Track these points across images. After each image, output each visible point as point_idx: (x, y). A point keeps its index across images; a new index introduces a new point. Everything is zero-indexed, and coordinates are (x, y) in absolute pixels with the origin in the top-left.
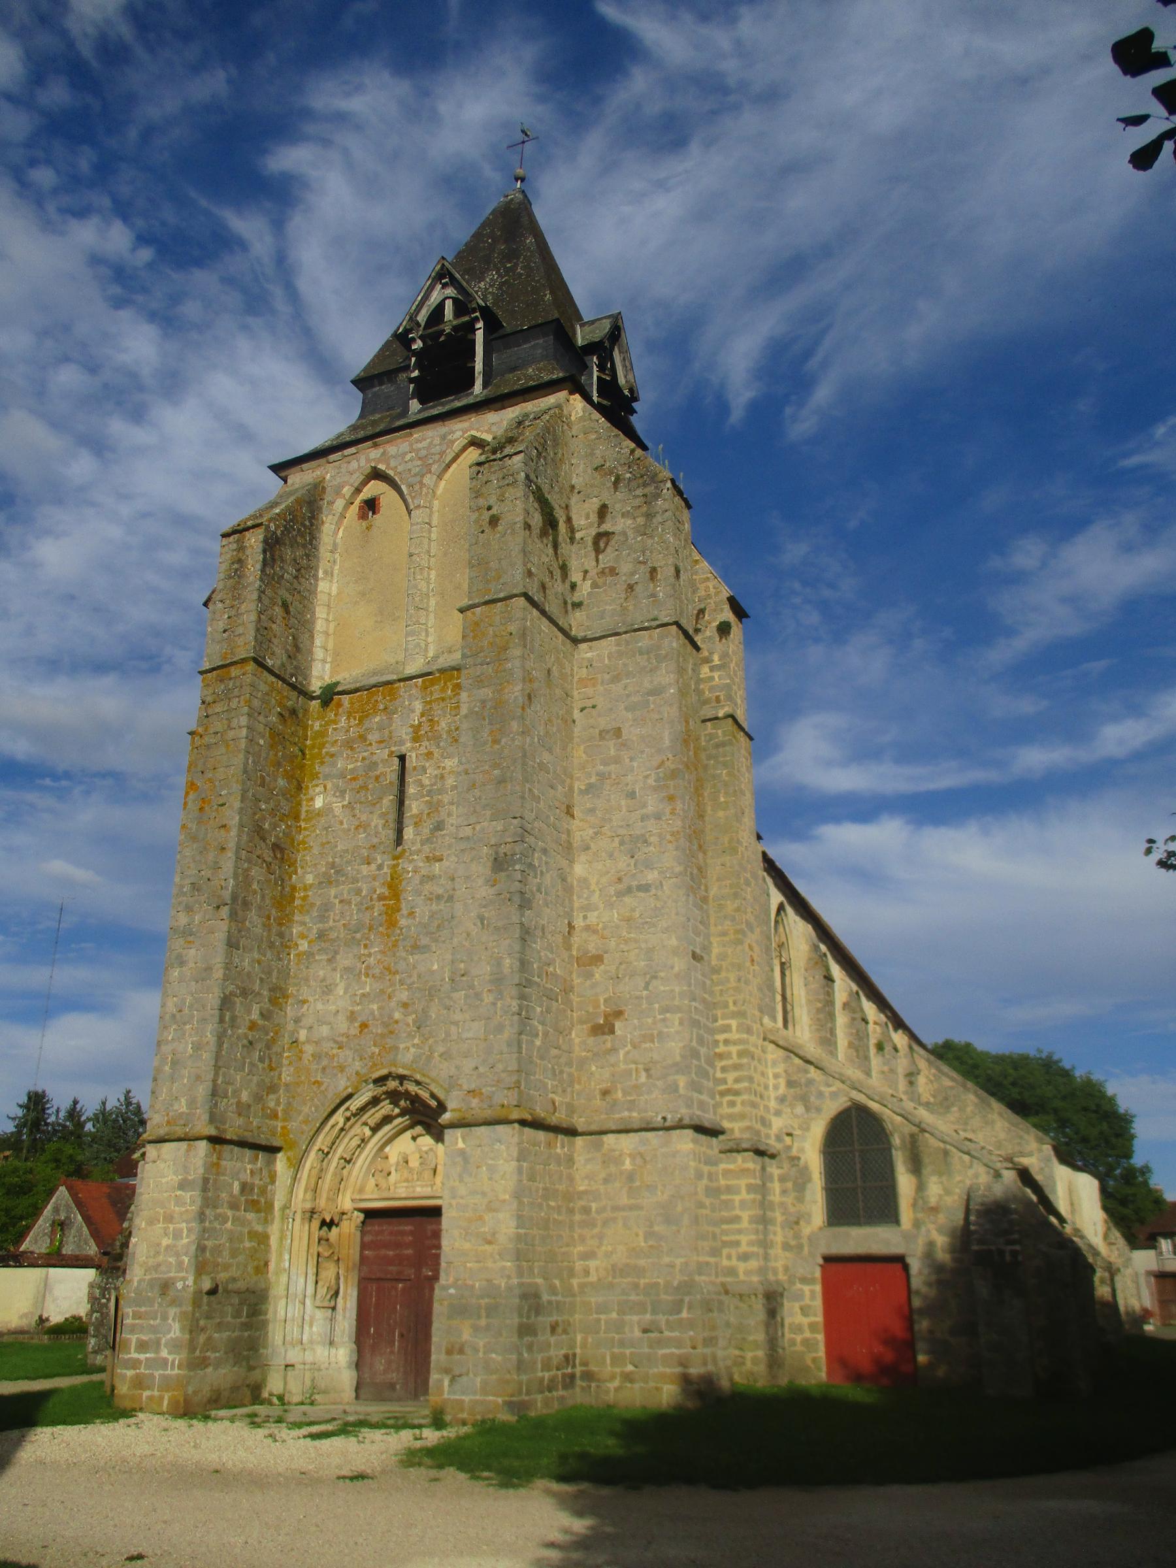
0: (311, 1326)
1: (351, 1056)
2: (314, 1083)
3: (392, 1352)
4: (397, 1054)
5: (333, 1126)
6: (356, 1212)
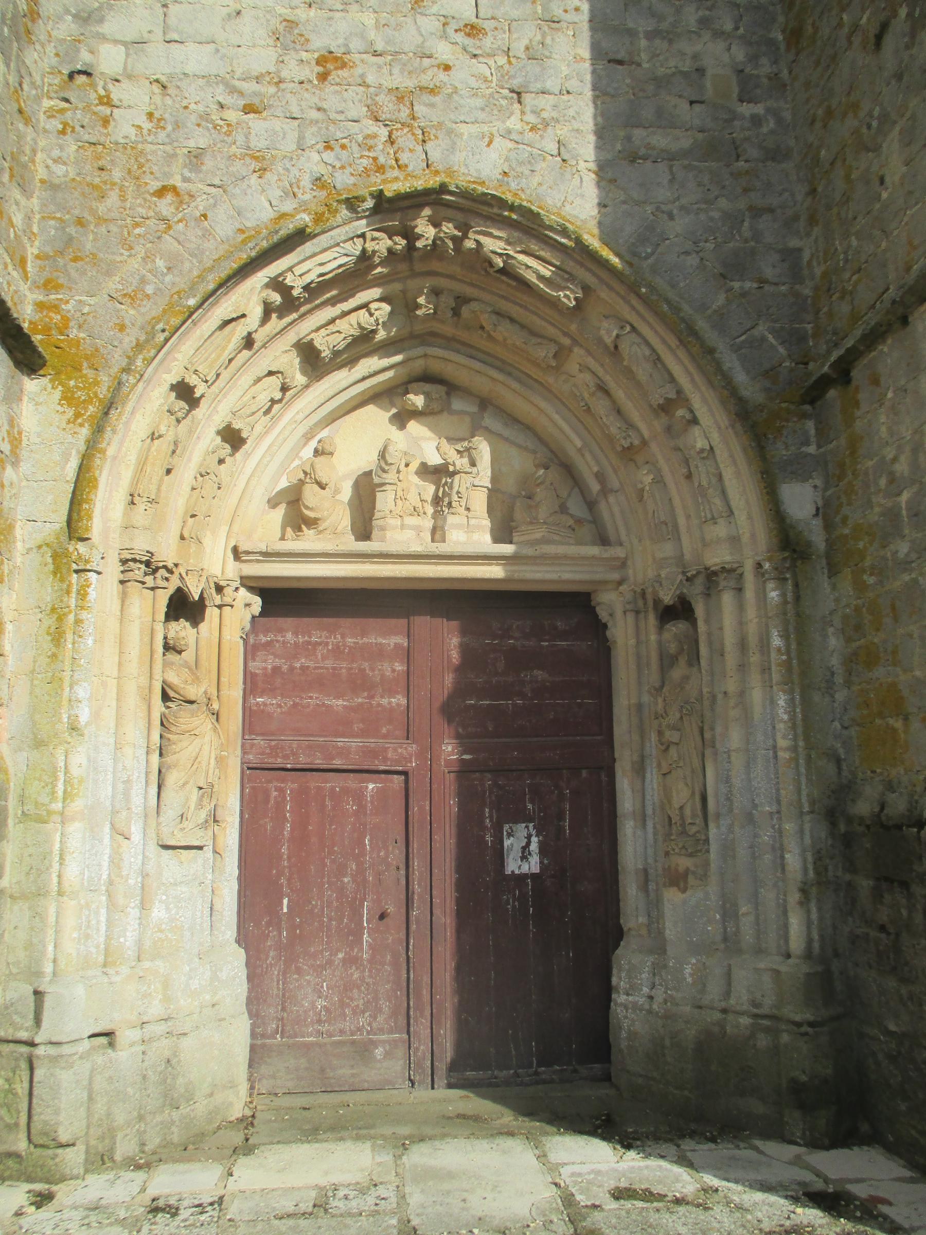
1: (293, 136)
2: (161, 192)
3: (352, 961)
4: (453, 148)
6: (242, 591)
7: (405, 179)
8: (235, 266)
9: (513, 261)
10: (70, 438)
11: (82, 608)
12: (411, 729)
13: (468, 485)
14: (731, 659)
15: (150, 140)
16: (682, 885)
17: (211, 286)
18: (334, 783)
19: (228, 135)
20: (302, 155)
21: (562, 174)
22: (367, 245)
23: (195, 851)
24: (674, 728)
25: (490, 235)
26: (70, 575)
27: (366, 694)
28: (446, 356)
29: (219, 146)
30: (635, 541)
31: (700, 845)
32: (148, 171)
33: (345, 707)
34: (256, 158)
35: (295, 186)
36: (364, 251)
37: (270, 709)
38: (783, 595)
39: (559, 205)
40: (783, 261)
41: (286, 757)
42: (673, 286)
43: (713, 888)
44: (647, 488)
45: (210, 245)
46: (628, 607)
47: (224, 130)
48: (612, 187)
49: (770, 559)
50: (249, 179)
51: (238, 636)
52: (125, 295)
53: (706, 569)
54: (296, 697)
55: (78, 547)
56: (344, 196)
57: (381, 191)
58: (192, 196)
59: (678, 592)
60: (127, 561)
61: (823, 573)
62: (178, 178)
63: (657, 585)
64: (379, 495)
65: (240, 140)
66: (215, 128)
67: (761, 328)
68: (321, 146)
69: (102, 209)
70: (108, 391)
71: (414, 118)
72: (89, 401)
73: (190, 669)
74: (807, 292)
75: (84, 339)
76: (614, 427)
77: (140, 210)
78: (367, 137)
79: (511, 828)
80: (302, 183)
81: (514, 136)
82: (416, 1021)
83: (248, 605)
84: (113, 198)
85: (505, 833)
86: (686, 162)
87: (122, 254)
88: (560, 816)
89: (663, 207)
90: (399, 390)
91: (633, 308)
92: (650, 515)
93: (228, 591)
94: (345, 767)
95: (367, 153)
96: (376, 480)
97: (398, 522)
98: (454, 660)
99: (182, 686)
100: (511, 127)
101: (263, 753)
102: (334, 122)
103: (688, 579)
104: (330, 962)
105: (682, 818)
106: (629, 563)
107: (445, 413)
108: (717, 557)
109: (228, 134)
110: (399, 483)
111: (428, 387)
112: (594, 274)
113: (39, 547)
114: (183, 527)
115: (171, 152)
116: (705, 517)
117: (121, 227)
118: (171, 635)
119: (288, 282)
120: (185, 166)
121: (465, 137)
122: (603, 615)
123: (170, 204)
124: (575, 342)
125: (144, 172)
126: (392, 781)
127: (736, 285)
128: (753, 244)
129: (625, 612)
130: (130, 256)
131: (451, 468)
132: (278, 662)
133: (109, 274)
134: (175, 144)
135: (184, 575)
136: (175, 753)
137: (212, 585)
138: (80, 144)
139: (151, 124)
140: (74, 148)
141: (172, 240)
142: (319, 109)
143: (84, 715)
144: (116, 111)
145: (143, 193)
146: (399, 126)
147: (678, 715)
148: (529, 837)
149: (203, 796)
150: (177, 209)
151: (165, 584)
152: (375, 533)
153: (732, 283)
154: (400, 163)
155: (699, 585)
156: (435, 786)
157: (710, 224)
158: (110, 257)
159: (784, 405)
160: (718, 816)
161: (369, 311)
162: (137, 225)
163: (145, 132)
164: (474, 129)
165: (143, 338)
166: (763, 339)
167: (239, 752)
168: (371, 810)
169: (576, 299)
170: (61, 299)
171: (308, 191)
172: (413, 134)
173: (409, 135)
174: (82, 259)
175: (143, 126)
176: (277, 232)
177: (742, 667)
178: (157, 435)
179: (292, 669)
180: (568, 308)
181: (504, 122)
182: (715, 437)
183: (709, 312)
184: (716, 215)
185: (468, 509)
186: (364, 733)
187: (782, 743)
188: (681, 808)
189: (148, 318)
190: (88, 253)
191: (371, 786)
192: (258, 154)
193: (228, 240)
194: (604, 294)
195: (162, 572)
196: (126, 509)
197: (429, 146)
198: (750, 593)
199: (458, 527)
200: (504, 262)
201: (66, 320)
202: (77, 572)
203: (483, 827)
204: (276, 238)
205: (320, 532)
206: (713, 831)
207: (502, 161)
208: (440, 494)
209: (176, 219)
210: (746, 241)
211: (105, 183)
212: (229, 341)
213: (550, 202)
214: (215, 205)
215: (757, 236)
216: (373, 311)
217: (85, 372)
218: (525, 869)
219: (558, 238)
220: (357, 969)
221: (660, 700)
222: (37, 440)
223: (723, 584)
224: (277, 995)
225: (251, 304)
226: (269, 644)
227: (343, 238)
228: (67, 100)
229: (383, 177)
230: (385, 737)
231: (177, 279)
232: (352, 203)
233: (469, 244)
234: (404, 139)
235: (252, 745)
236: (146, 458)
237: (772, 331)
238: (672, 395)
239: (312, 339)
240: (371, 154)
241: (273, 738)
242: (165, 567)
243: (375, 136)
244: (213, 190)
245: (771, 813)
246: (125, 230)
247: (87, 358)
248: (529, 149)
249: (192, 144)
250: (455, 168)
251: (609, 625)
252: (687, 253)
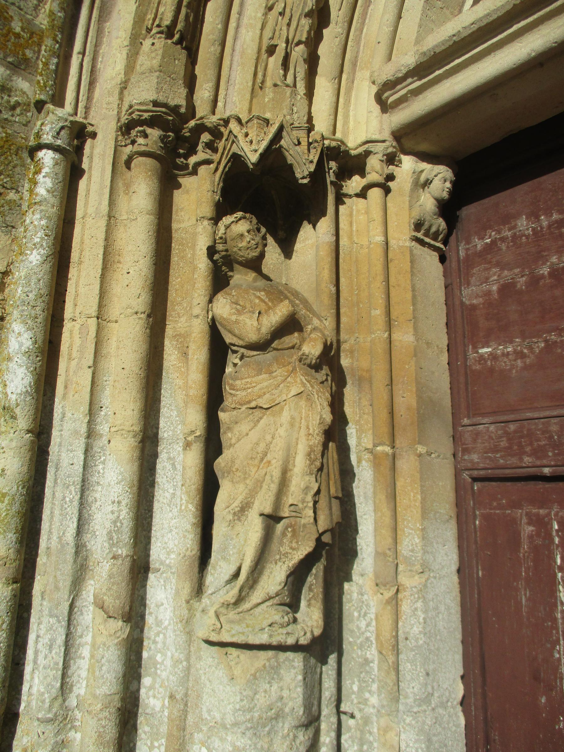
23: (270, 653)
37: (505, 364)
41: (538, 453)
51: (407, 237)
54: (549, 332)
99: (234, 318)
101: (495, 450)
179: (535, 280)
226: (491, 248)
241: (512, 417)
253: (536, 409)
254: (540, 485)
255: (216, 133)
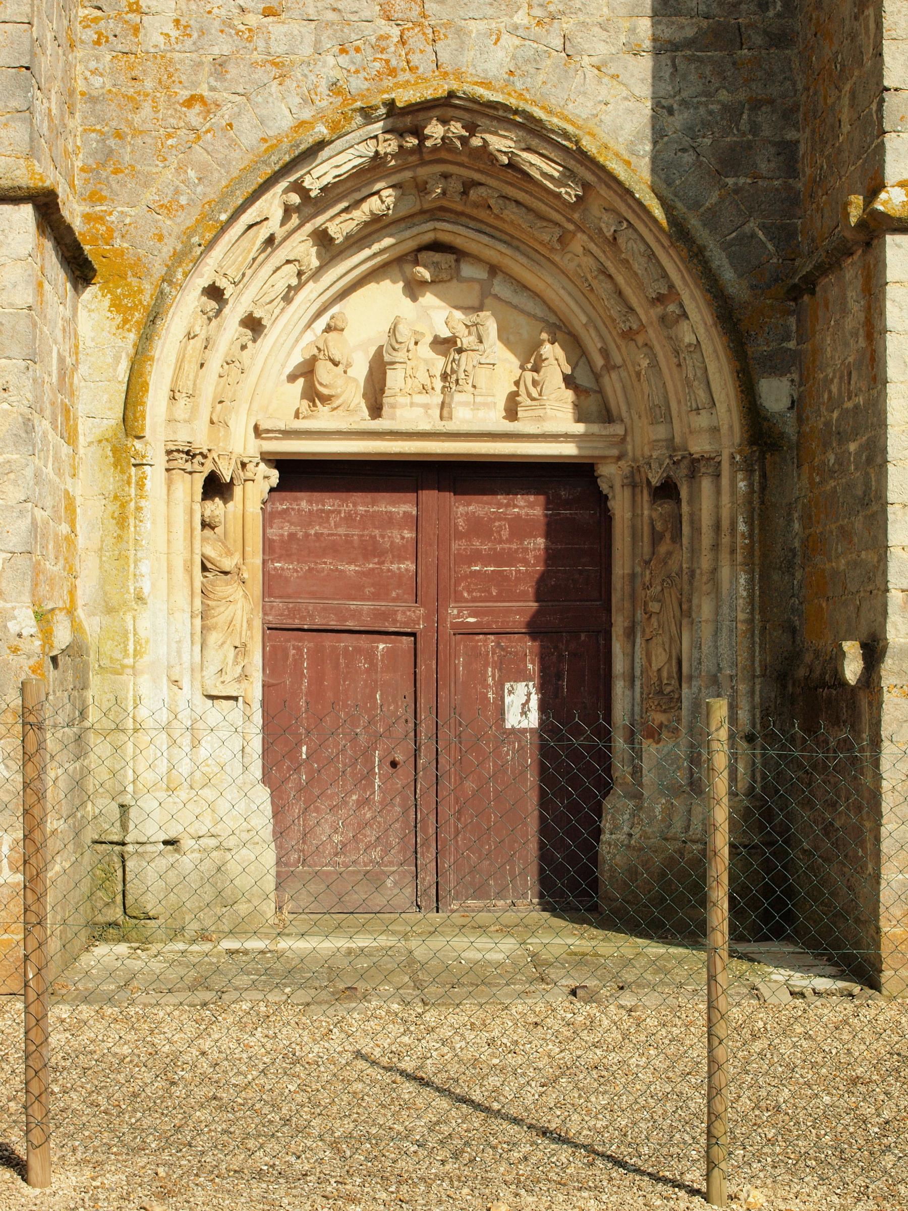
0: (196, 744)
1: (310, 39)
2: (190, 102)
4: (462, 47)
5: (250, 227)
6: (262, 465)
7: (416, 83)
8: (261, 181)
9: (518, 159)
10: (119, 343)
11: (141, 497)
12: (419, 593)
13: (475, 363)
14: (706, 540)
15: (177, 49)
16: (656, 738)
17: (240, 201)
18: (347, 641)
19: (250, 41)
20: (319, 60)
21: (566, 71)
22: (379, 149)
24: (655, 599)
25: (495, 133)
26: (130, 468)
27: (376, 560)
28: (454, 230)
29: (241, 52)
30: (636, 417)
31: (672, 702)
32: (177, 80)
33: (356, 572)
34: (275, 64)
35: (312, 92)
36: (377, 152)
37: (287, 574)
38: (751, 485)
39: (562, 103)
40: (779, 154)
41: (303, 618)
42: (669, 185)
43: (684, 739)
44: (643, 372)
45: (236, 154)
46: (625, 481)
47: (246, 36)
48: (615, 83)
49: (740, 452)
50: (271, 86)
52: (162, 206)
53: (691, 455)
54: (311, 562)
55: (135, 443)
56: (359, 104)
57: (393, 100)
58: (218, 105)
59: (665, 475)
60: (172, 451)
61: (793, 463)
62: (205, 86)
63: (646, 467)
64: (390, 374)
65: (261, 44)
66: (237, 34)
67: (752, 225)
68: (336, 49)
69: (137, 120)
70: (151, 298)
71: (425, 17)
72: (135, 308)
73: (223, 543)
74: (799, 186)
75: (127, 249)
76: (615, 310)
77: (172, 121)
78: (380, 38)
79: (512, 686)
80: (319, 90)
81: (521, 32)
82: (423, 855)
83: (266, 477)
84: (147, 109)
85: (506, 691)
86: (689, 53)
87: (157, 166)
88: (559, 676)
89: (663, 101)
90: (409, 258)
91: (630, 207)
92: (646, 397)
93: (250, 467)
94: (357, 628)
95: (379, 56)
96: (387, 358)
97: (408, 400)
98: (460, 528)
100: (519, 22)
101: (281, 615)
102: (348, 23)
103: (674, 463)
104: (345, 803)
105: (660, 679)
106: (629, 439)
107: (455, 281)
108: (699, 446)
109: (250, 40)
110: (408, 362)
111: (437, 257)
112: (594, 173)
113: (100, 441)
114: (212, 414)
115: (198, 60)
116: (691, 406)
117: (155, 137)
118: (207, 513)
119: (306, 184)
120: (211, 75)
121: (473, 35)
122: (604, 487)
123: (199, 114)
124: (579, 228)
125: (174, 82)
126: (401, 642)
127: (730, 181)
128: (750, 137)
129: (623, 486)
130: (164, 167)
131: (459, 345)
132: (293, 529)
133: (146, 185)
134: (201, 52)
135: (217, 459)
136: (214, 617)
137: (240, 466)
138: (114, 54)
139: (178, 32)
140: (108, 57)
141: (202, 151)
142: (334, 10)
143: (146, 587)
144: (145, 18)
145: (174, 104)
146: (410, 25)
147: (659, 588)
148: (529, 694)
149: (237, 654)
150: (205, 119)
151: (199, 468)
152: (386, 411)
153: (727, 180)
154: (411, 64)
155: (683, 470)
156: (440, 648)
157: (710, 118)
158: (147, 168)
159: (768, 302)
160: (690, 678)
161: (380, 198)
162: (169, 136)
163: (173, 40)
164: (482, 26)
165: (179, 247)
166: (753, 235)
167: (261, 615)
168: (381, 668)
169: (576, 196)
170: (106, 211)
171: (325, 97)
172: (424, 34)
173: (420, 35)
174: (122, 172)
175: (171, 34)
176: (298, 146)
177: (716, 547)
178: (192, 335)
179: (307, 535)
180: (569, 203)
181: (511, 17)
182: (701, 331)
183: (702, 210)
184: (715, 107)
185: (474, 387)
186: (375, 597)
187: (741, 616)
188: (659, 670)
189: (183, 228)
190: (126, 165)
191: (381, 646)
192: (278, 60)
193: (252, 149)
194: (603, 191)
195: (199, 458)
196: (168, 403)
197: (439, 46)
198: (725, 481)
199: (465, 404)
200: (509, 159)
201: (110, 230)
202: (135, 465)
203: (487, 686)
204: (297, 153)
205: (334, 409)
206: (685, 690)
207: (508, 59)
208: (449, 371)
209: (204, 129)
210: (744, 134)
211: (139, 93)
212: (254, 244)
213: (553, 101)
214: (239, 114)
215: (755, 128)
216: (384, 199)
217: (129, 280)
218: (524, 724)
219: (559, 140)
220: (370, 809)
221: (648, 572)
222: (92, 345)
223: (703, 470)
224: (299, 831)
225: (274, 207)
226: (285, 511)
227: (358, 141)
228: (99, 8)
229: (395, 80)
230: (394, 600)
231: (208, 190)
232: (367, 114)
233: (476, 142)
234: (416, 40)
235: (272, 607)
236: (184, 356)
237: (763, 227)
238: (664, 291)
239: (327, 228)
240: (384, 57)
241: (291, 600)
242: (201, 454)
243: (387, 37)
244: (237, 98)
245: (731, 676)
246: (159, 141)
247: (131, 267)
248: (535, 45)
249: (216, 51)
250: (463, 70)
251: (610, 496)
252: (684, 150)
253: (301, 598)
254: (300, 633)
255: (205, 457)
